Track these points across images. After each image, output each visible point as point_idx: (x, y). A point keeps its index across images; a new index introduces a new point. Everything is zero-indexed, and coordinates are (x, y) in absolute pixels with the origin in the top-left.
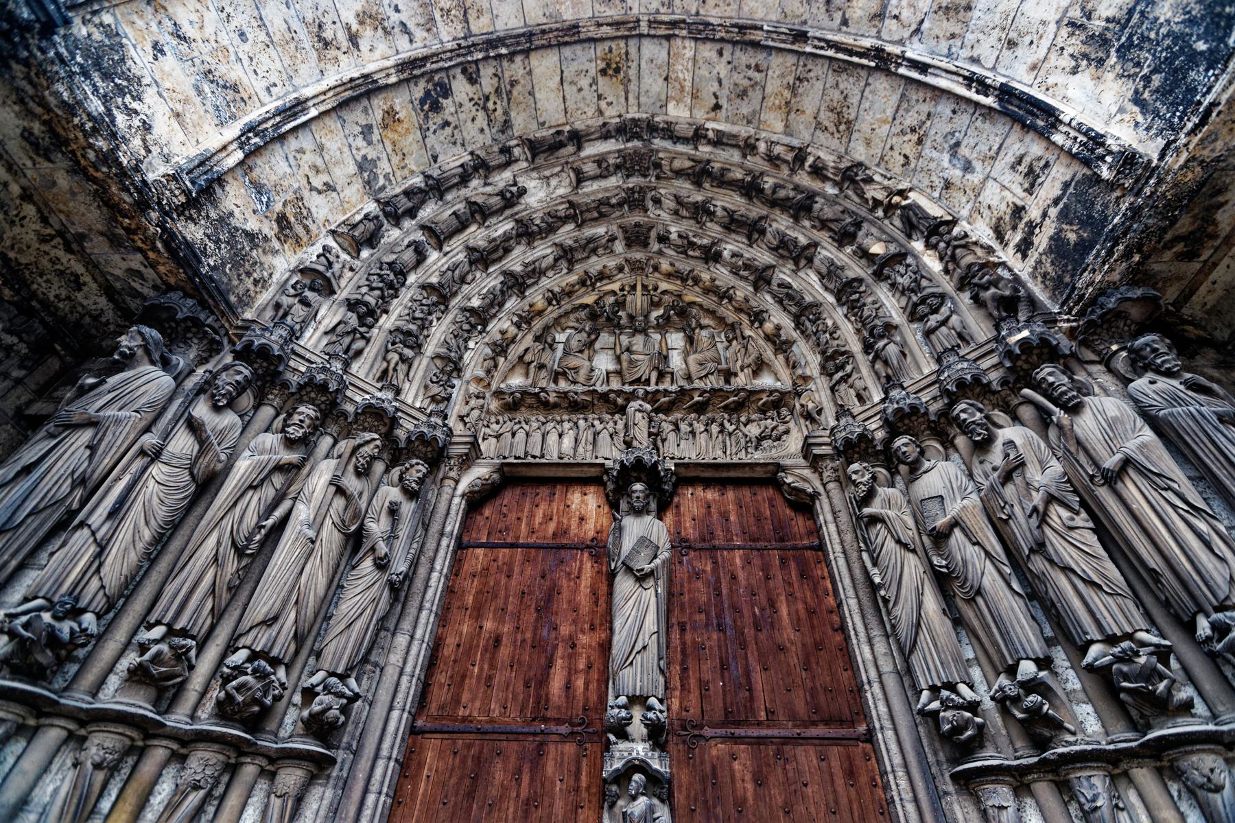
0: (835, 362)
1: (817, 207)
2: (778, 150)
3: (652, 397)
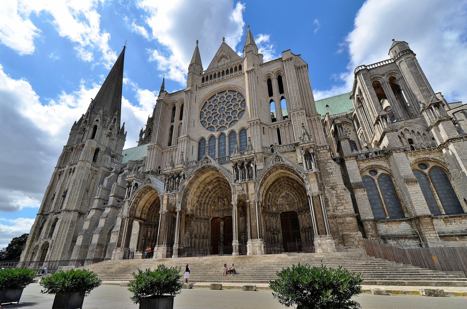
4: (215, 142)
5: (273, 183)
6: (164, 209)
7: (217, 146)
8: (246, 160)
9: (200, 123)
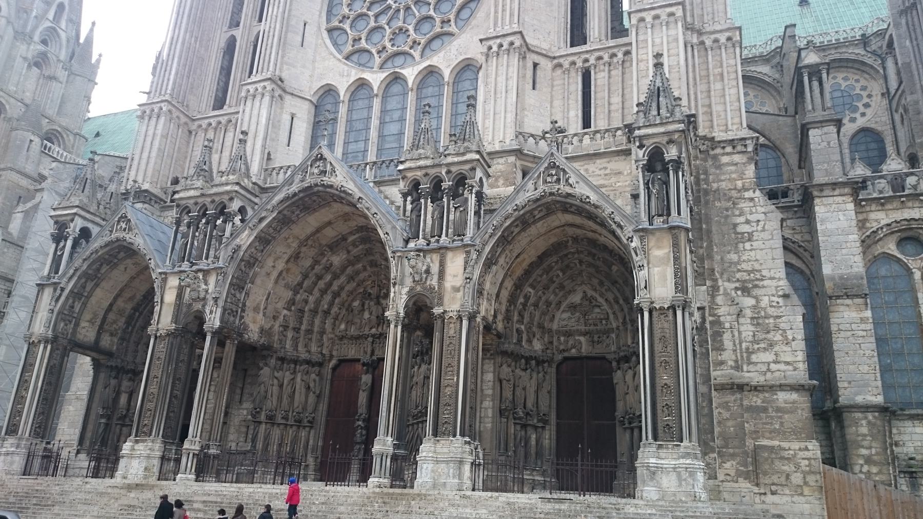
3: (373, 336)
4: (370, 107)
5: (542, 258)
6: (164, 319)
7: (375, 122)
8: (448, 172)
9: (325, 34)
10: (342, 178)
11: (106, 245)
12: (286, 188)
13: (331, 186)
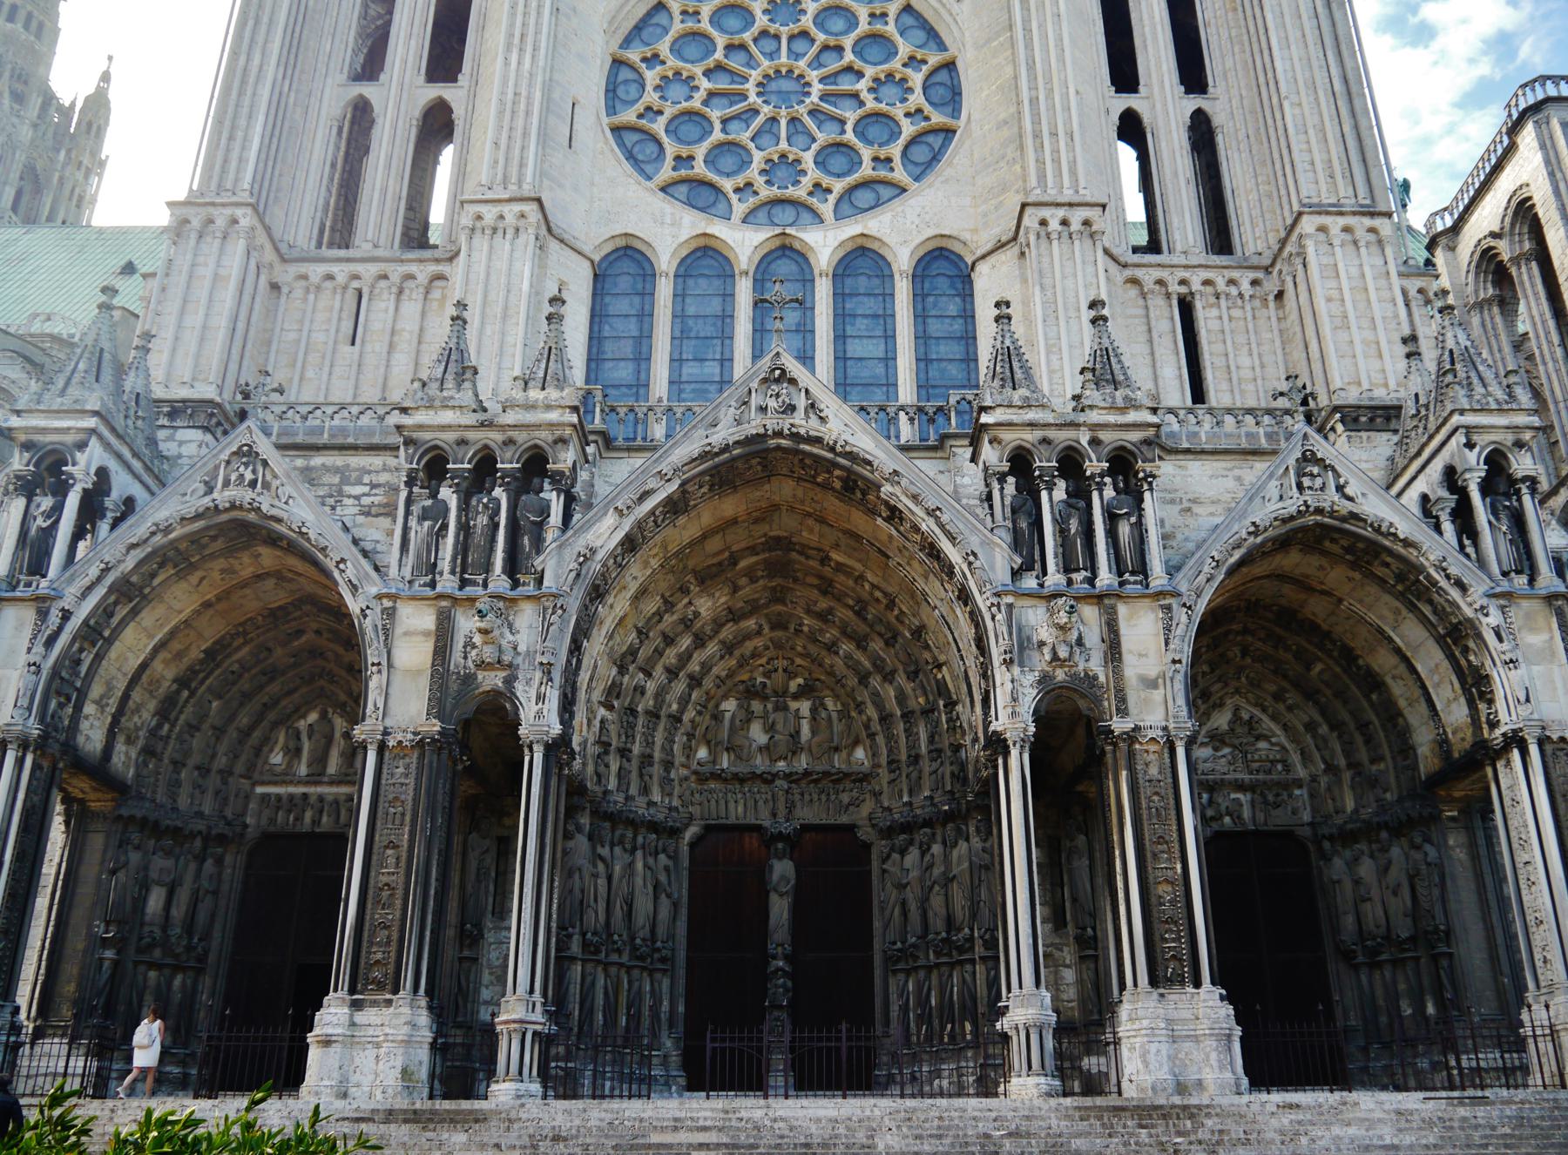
0: (893, 763)
1: (897, 646)
2: (878, 594)
3: (787, 776)
8: (1095, 442)
10: (843, 426)
11: (198, 516)
12: (701, 432)
13: (818, 441)
